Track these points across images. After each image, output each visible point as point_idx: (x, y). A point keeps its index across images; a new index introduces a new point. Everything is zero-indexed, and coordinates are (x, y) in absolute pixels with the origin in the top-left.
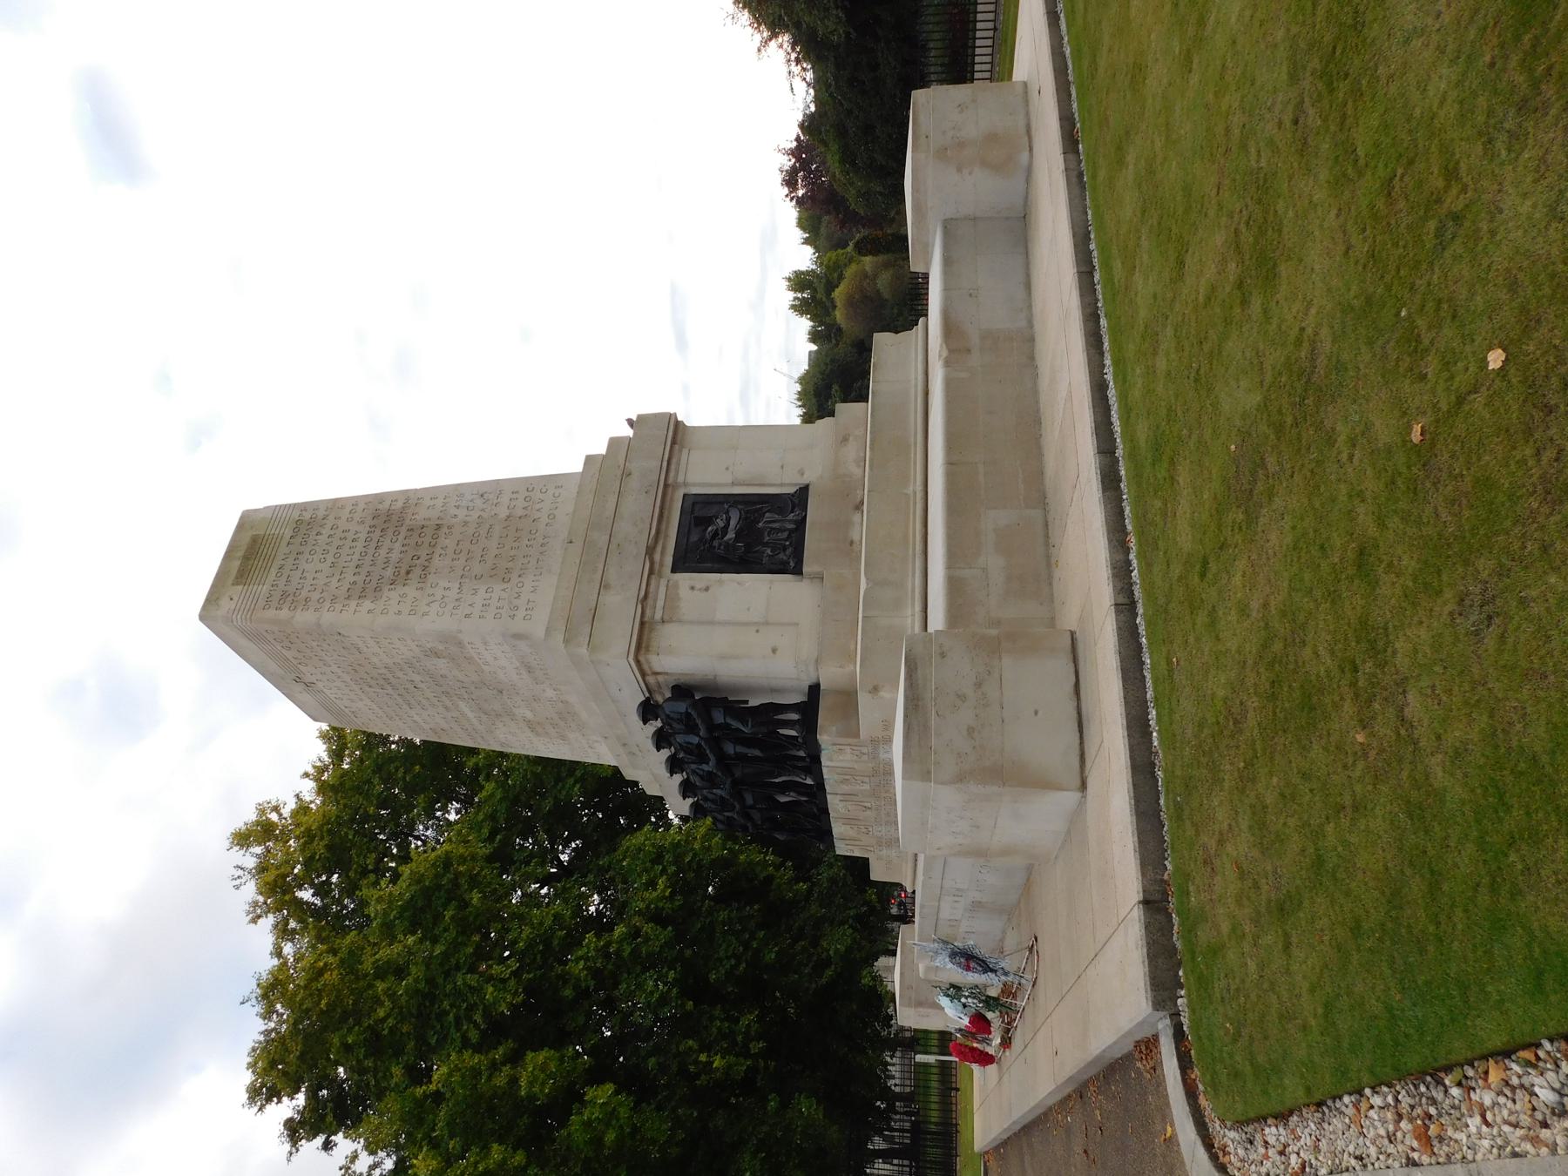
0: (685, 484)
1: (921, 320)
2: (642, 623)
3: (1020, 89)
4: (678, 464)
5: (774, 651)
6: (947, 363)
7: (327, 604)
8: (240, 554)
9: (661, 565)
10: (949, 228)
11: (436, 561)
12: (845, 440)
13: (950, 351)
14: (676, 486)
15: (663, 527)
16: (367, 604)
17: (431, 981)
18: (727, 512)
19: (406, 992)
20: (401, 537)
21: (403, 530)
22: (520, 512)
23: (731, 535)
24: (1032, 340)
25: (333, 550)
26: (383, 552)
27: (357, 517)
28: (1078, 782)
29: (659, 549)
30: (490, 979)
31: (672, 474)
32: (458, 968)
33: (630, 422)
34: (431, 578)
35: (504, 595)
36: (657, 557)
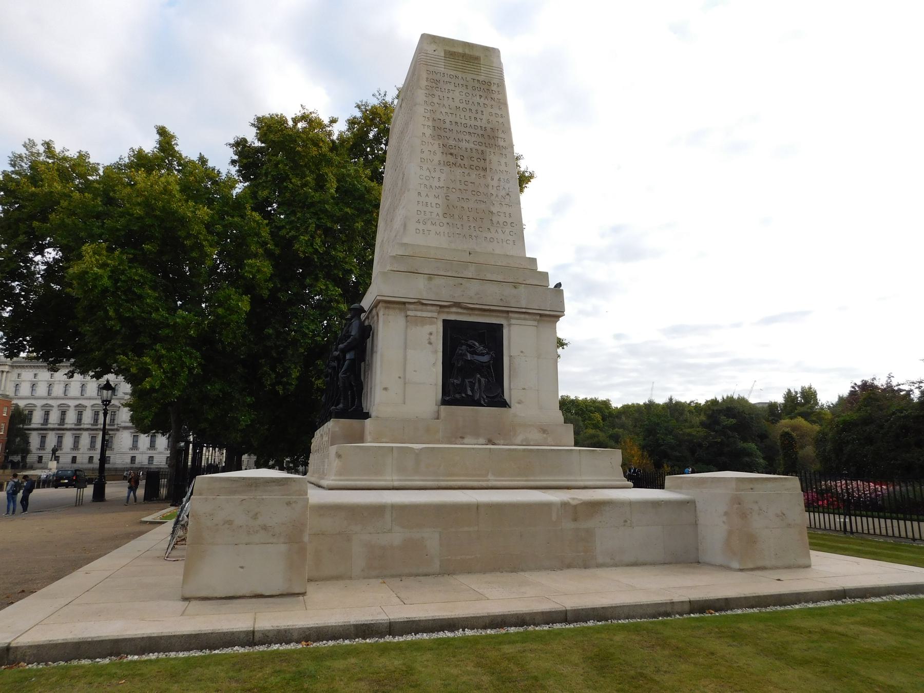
0: (510, 325)
1: (631, 484)
2: (404, 303)
3: (802, 561)
4: (525, 319)
5: (385, 389)
6: (564, 505)
7: (429, 108)
8: (467, 51)
9: (448, 313)
10: (688, 505)
11: (459, 171)
13: (575, 507)
14: (508, 319)
15: (476, 312)
16: (428, 132)
17: (313, 204)
18: (487, 353)
19: (305, 192)
20: (477, 147)
21: (483, 148)
22: (495, 219)
23: (469, 357)
24: (586, 567)
25: (468, 107)
26: (467, 137)
27: (491, 118)
28: (188, 595)
29: (460, 310)
30: (313, 237)
32: (319, 219)
33: (559, 285)
34: (446, 169)
35: (434, 215)
36: (454, 310)
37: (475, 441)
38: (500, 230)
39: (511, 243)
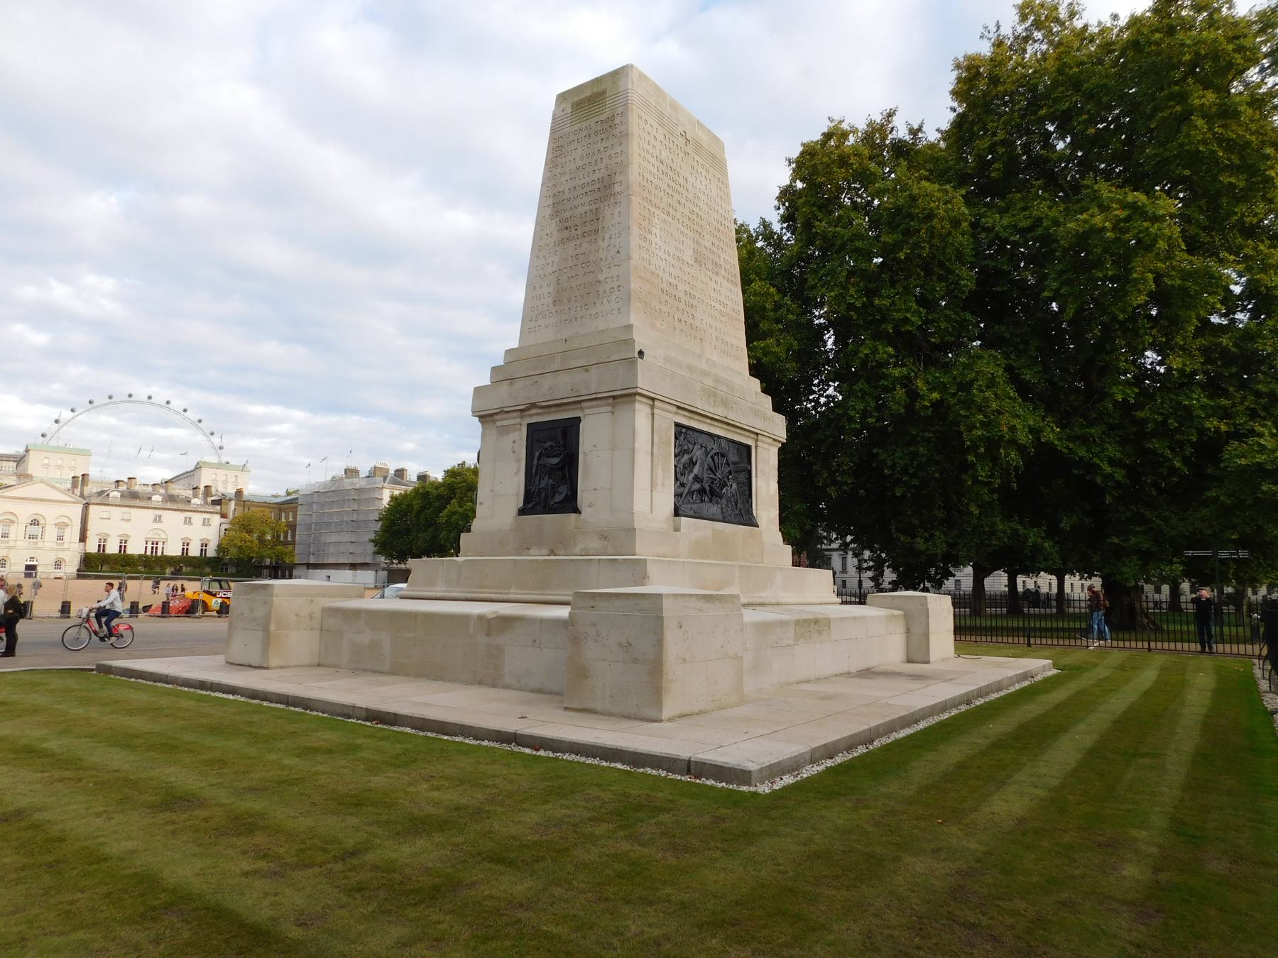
3: (652, 713)
4: (598, 406)
6: (481, 618)
8: (595, 90)
9: (531, 415)
13: (490, 621)
24: (494, 686)
29: (539, 411)
36: (533, 411)
39: (615, 312)
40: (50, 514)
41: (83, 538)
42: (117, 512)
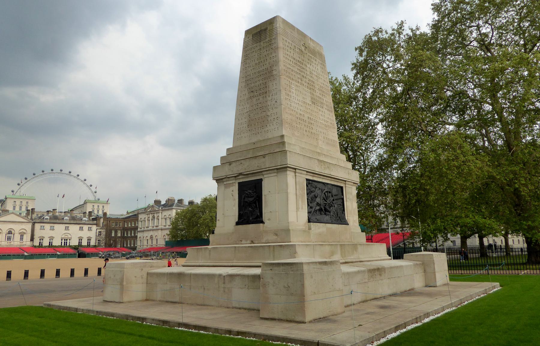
4: (270, 173)
9: (239, 179)
12: (276, 235)
29: (243, 176)
31: (265, 173)
36: (241, 177)
37: (246, 242)
38: (271, 124)
39: (276, 129)
40: (17, 228)
41: (32, 239)
42: (47, 226)
